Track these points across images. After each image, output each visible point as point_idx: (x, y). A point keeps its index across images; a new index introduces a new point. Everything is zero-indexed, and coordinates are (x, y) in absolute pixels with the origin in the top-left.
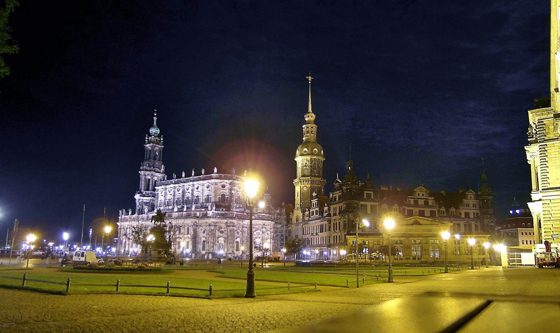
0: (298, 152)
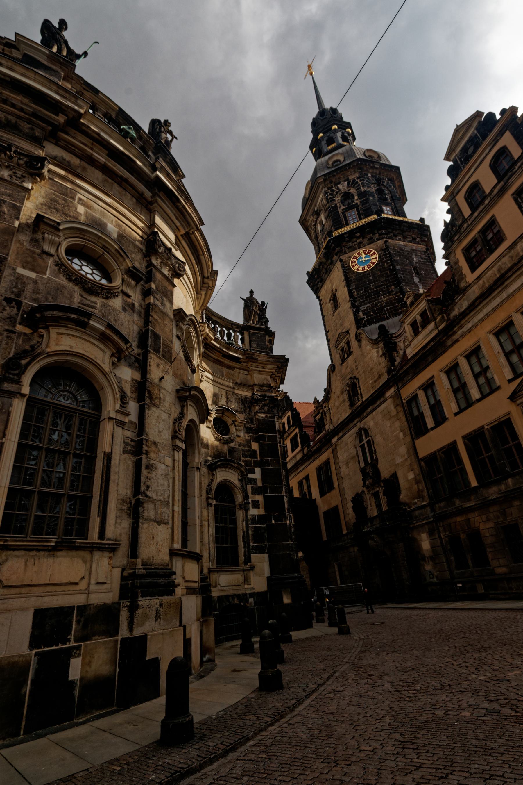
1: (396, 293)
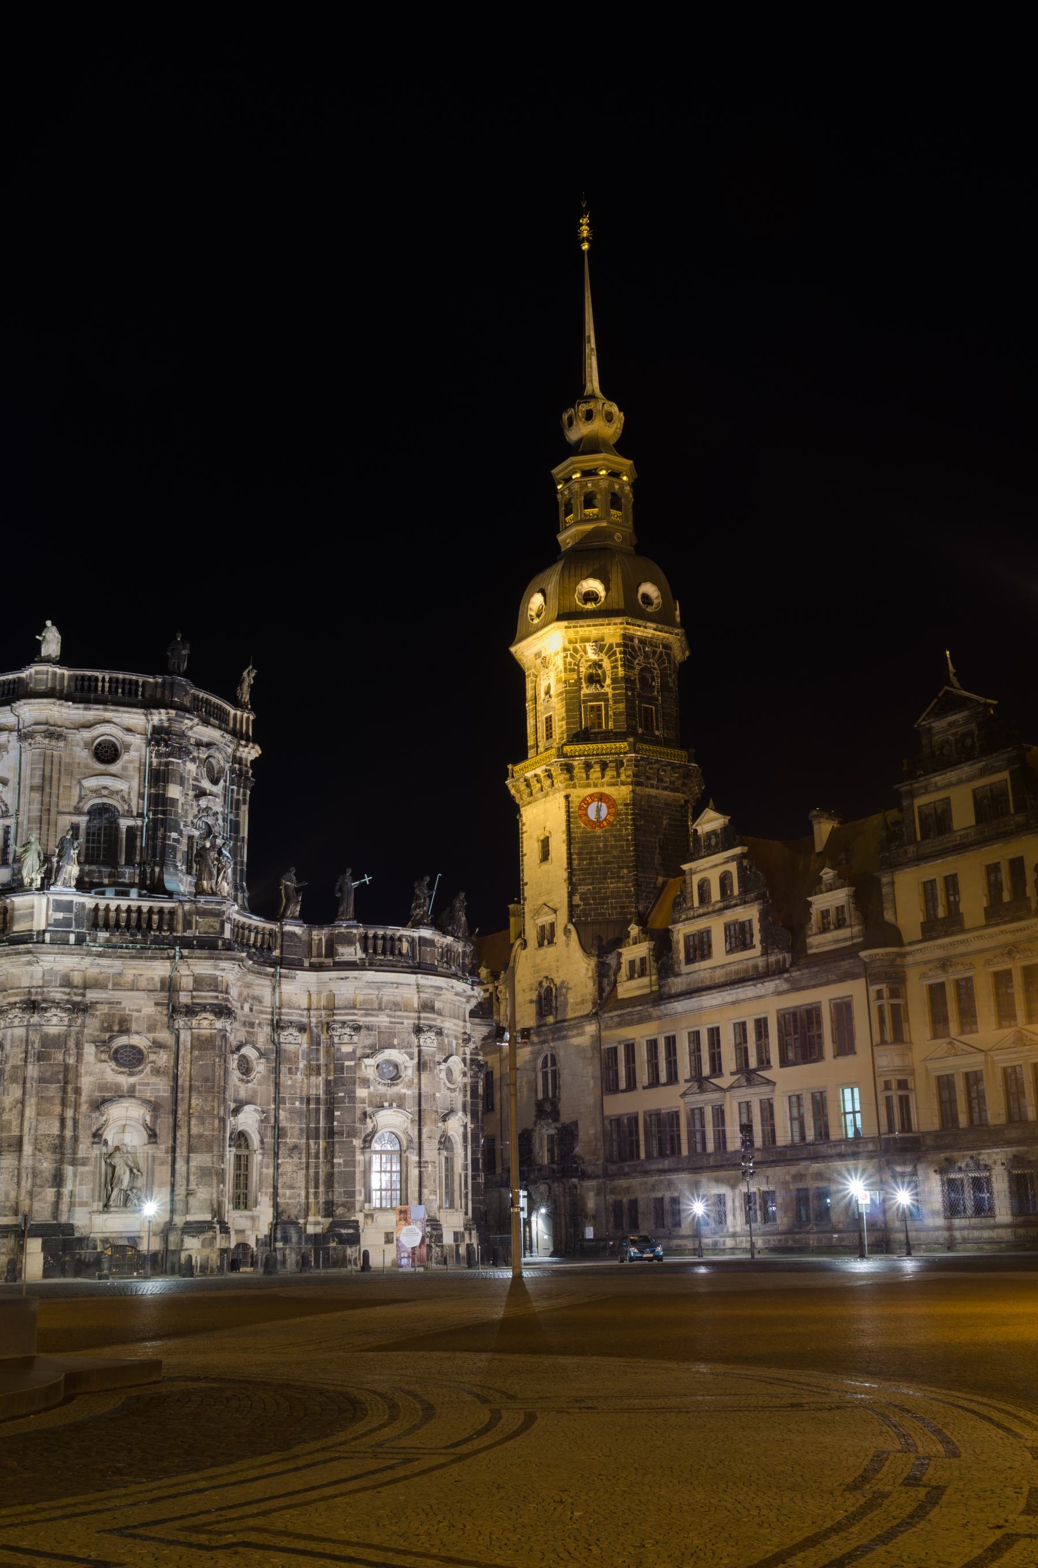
0: (537, 600)
1: (627, 882)
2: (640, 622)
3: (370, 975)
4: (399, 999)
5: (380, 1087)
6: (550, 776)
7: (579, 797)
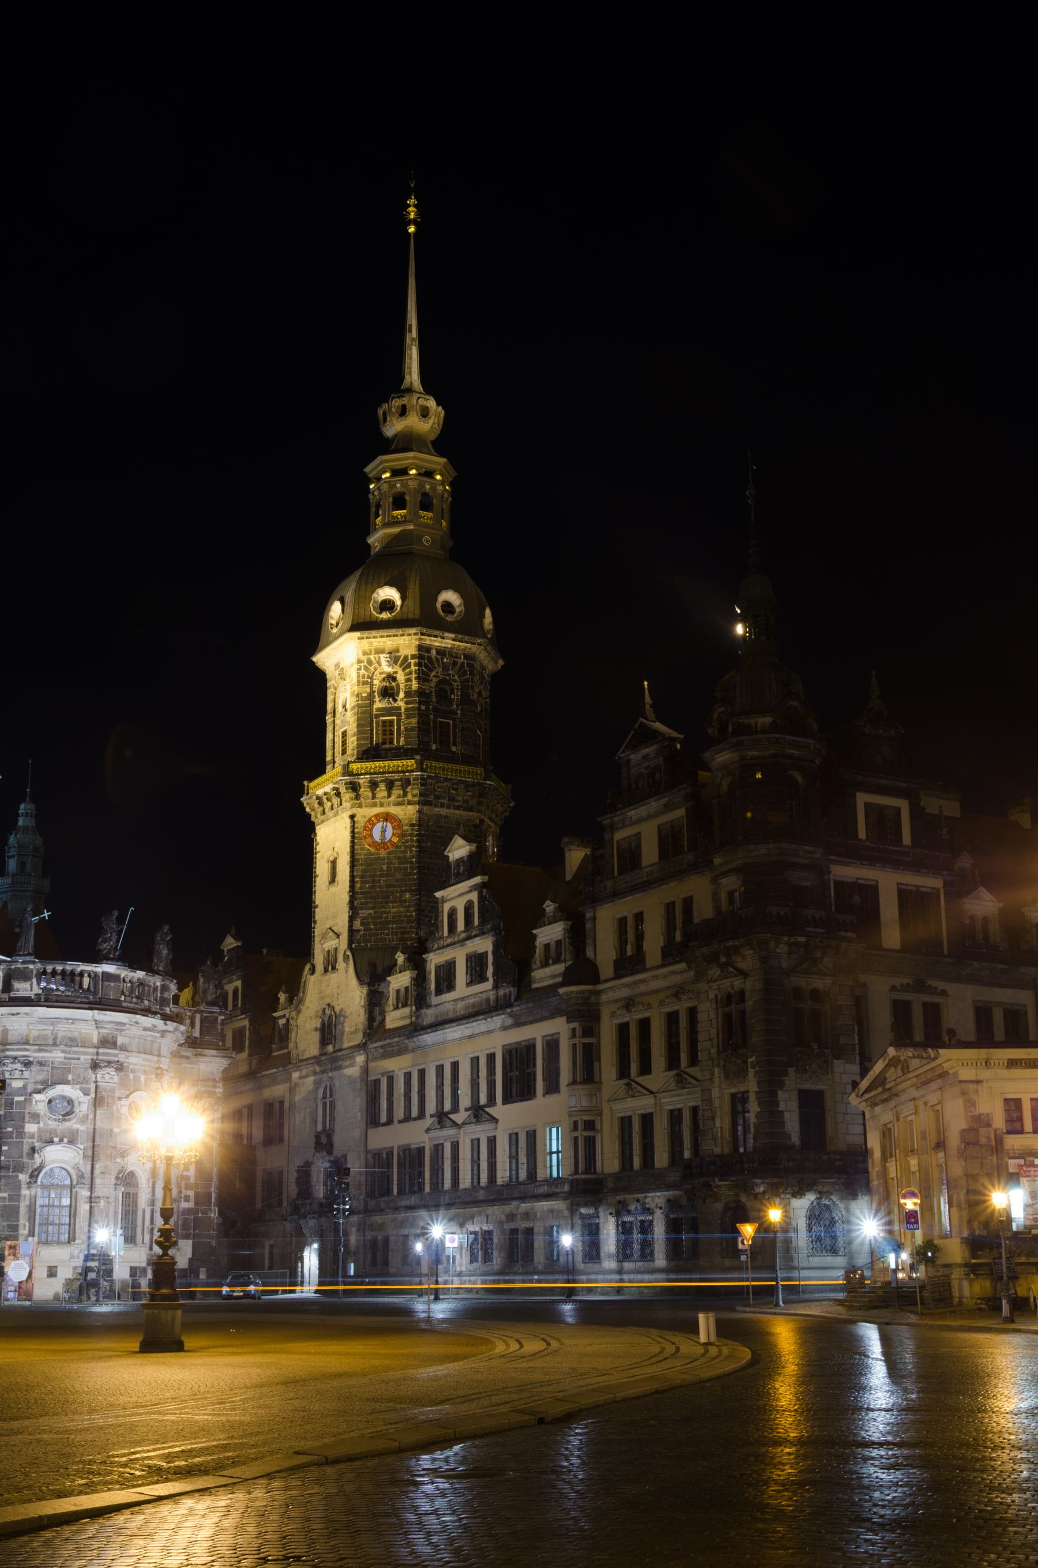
0: (336, 610)
1: (409, 907)
2: (435, 632)
3: (41, 1011)
4: (76, 1034)
5: (50, 1122)
6: (338, 794)
7: (365, 817)
